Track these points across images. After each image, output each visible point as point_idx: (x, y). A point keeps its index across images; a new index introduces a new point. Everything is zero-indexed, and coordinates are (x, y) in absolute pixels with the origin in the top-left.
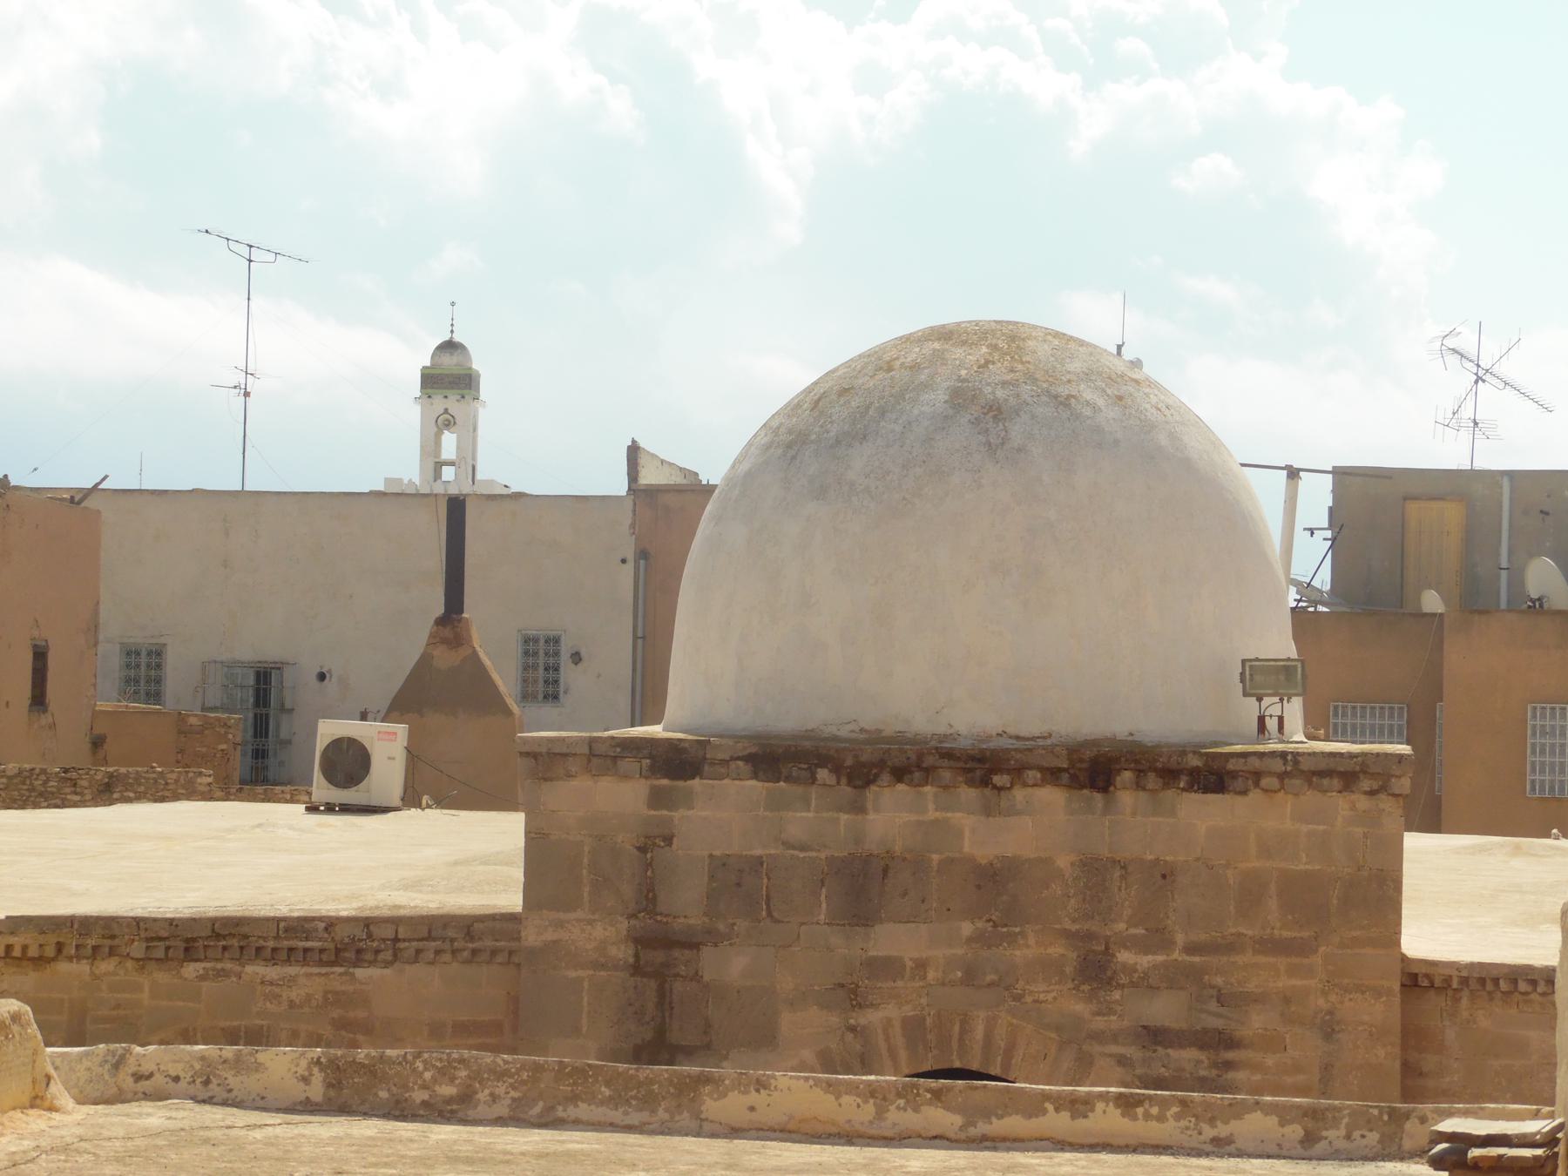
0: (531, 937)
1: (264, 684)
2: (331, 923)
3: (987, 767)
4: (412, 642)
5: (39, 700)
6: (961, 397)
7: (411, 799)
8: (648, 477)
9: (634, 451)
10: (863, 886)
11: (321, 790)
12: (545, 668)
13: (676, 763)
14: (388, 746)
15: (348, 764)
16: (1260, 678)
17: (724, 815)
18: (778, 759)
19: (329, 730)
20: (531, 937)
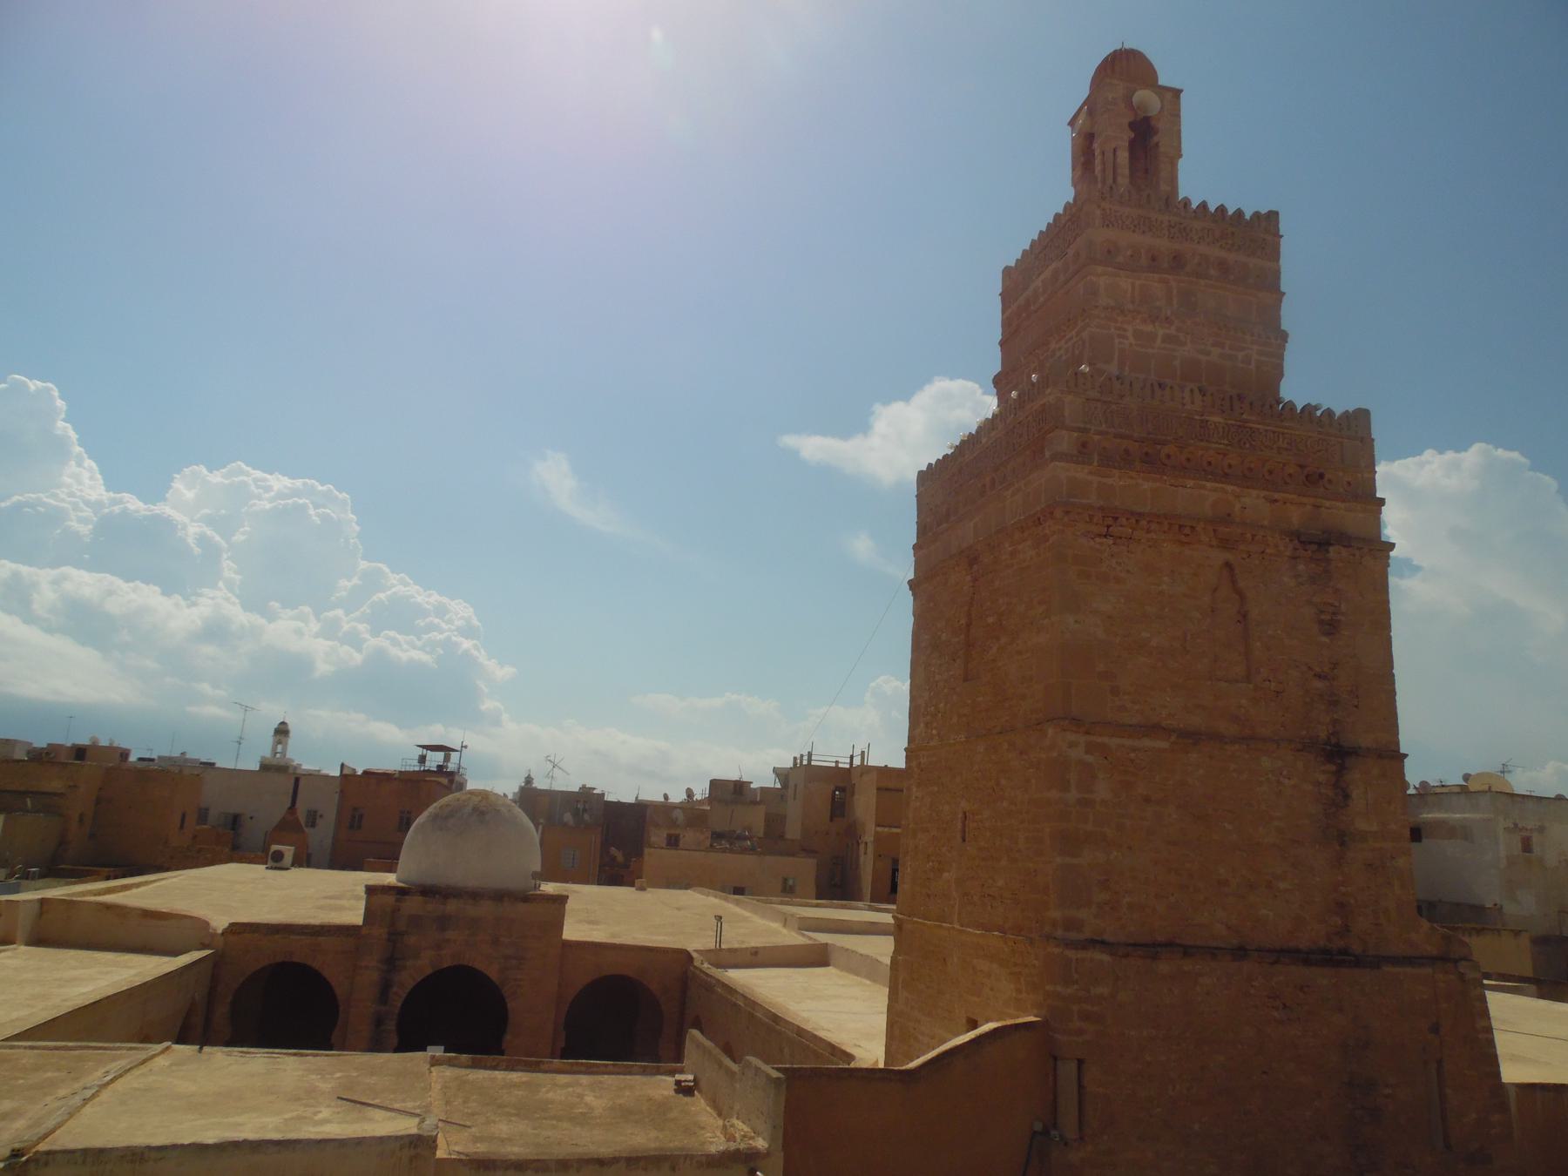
0: (364, 931)
1: (235, 821)
2: (314, 927)
3: (475, 895)
4: (279, 813)
5: (182, 827)
6: (475, 809)
7: (293, 865)
8: (346, 772)
9: (342, 765)
10: (443, 922)
11: (270, 863)
12: (313, 818)
13: (400, 892)
14: (289, 851)
15: (278, 857)
16: (536, 876)
17: (413, 905)
18: (427, 891)
19: (275, 847)
20: (364, 931)
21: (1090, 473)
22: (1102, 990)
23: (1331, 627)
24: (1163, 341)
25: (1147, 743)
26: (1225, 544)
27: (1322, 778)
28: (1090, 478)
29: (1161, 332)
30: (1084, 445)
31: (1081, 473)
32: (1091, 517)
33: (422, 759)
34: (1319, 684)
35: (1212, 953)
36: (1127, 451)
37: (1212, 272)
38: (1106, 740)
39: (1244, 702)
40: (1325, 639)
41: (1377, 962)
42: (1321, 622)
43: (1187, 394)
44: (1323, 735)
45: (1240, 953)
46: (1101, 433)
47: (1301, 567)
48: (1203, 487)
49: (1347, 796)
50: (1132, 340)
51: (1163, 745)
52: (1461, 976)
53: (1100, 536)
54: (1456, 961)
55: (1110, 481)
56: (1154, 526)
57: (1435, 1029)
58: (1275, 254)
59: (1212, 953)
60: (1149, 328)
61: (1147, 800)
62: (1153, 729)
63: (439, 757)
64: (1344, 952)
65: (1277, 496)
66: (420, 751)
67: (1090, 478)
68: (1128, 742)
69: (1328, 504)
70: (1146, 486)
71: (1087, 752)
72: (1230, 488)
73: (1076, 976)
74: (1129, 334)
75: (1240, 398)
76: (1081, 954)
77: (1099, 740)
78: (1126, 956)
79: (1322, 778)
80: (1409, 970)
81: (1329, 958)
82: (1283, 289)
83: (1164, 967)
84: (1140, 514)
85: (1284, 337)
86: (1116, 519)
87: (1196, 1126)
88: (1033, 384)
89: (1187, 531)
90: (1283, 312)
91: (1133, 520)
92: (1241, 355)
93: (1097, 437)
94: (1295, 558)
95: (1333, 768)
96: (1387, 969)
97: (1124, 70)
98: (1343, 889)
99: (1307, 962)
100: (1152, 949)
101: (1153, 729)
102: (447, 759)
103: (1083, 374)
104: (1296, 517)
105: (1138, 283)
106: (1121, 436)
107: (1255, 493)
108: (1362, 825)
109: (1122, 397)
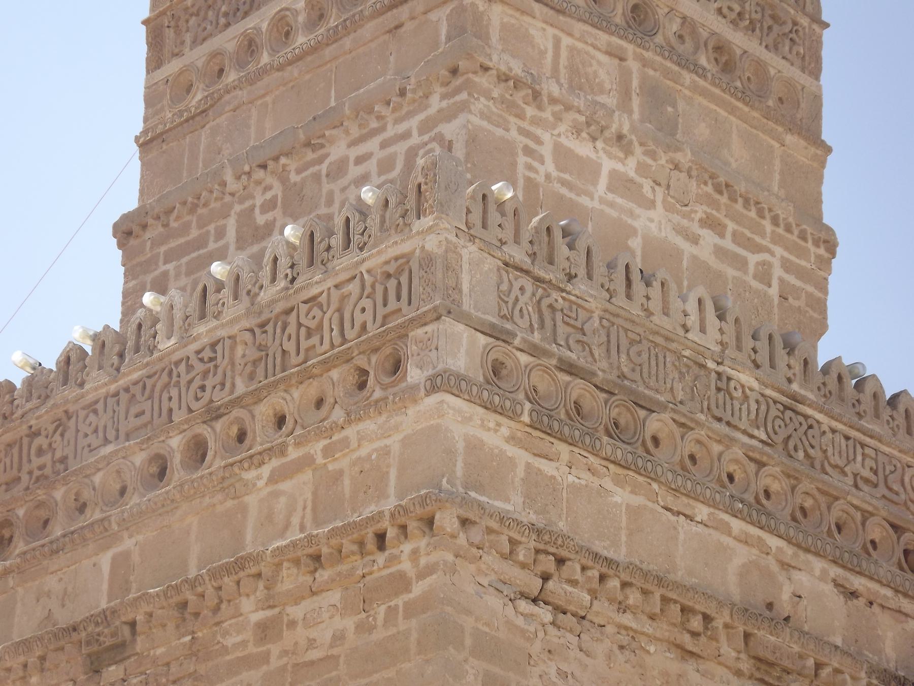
21: (512, 439)
24: (610, 189)
28: (511, 451)
30: (497, 369)
31: (495, 435)
32: (512, 541)
37: (703, 61)
43: (692, 306)
46: (534, 351)
53: (523, 595)
56: (634, 597)
58: (812, 64)
60: (583, 149)
65: (858, 583)
70: (621, 496)
72: (774, 542)
74: (546, 151)
75: (790, 348)
82: (827, 136)
84: (609, 562)
85: (830, 245)
86: (560, 561)
88: (363, 211)
89: (696, 623)
90: (825, 189)
91: (594, 573)
92: (753, 259)
93: (524, 358)
103: (501, 205)
105: (566, 41)
106: (569, 368)
107: (818, 565)
109: (571, 277)
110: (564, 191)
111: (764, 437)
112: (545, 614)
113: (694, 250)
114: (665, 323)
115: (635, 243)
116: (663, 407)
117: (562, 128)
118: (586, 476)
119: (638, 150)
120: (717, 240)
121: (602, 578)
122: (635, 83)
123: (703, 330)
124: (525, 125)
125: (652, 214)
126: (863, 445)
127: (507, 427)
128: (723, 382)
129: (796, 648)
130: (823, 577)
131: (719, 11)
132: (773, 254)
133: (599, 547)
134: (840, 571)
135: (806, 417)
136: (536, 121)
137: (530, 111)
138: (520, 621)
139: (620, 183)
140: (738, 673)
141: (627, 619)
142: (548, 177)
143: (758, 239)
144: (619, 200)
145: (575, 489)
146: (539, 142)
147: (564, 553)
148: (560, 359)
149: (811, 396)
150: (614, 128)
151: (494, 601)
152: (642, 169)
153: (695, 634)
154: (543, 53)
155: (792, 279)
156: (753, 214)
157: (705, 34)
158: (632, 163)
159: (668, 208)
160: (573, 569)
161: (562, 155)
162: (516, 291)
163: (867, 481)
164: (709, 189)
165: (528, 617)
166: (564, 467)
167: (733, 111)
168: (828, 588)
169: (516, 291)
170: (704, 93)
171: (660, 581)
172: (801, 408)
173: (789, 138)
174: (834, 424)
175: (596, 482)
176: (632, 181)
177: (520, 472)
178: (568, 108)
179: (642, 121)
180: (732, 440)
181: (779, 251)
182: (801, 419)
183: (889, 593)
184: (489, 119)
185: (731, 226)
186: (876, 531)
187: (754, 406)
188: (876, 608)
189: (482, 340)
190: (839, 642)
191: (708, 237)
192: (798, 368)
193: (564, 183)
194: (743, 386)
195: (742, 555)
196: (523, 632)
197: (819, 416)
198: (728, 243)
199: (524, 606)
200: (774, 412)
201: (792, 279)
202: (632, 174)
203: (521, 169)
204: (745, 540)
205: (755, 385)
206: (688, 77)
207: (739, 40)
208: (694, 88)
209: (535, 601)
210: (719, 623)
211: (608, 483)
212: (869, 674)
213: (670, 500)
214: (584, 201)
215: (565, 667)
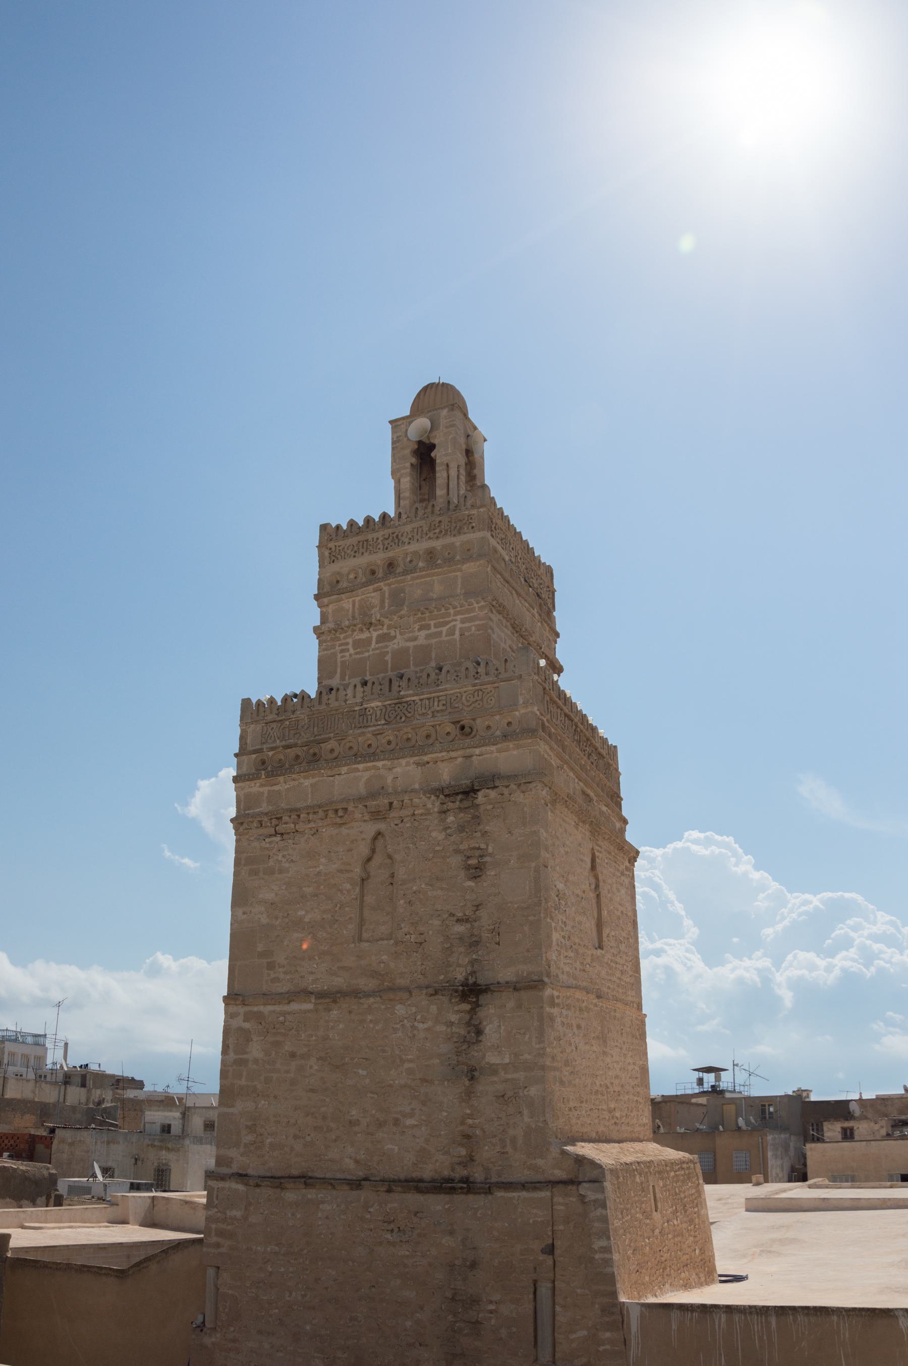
21: (262, 785)
22: (238, 1213)
23: (476, 871)
25: (295, 1006)
26: (377, 815)
27: (454, 1018)
28: (261, 790)
29: (375, 635)
33: (700, 1082)
34: (460, 928)
35: (330, 1183)
36: (297, 757)
38: (261, 1008)
39: (384, 957)
40: (471, 883)
41: (488, 1189)
42: (468, 868)
44: (460, 975)
45: (356, 1184)
46: (272, 749)
47: (451, 819)
48: (358, 770)
49: (479, 1032)
50: (352, 651)
51: (309, 1006)
52: (582, 1197)
54: (580, 1183)
55: (276, 788)
56: (311, 817)
57: (550, 1250)
59: (330, 1183)
61: (293, 1055)
62: (306, 993)
63: (709, 1079)
64: (466, 1180)
65: (426, 758)
66: (697, 1075)
67: (261, 790)
68: (278, 1008)
69: (477, 751)
70: (307, 783)
71: (244, 1021)
72: (380, 764)
73: (216, 1202)
74: (350, 647)
76: (221, 1184)
77: (255, 1009)
78: (258, 1186)
79: (454, 1018)
80: (524, 1194)
81: (443, 1186)
83: (290, 1196)
87: (308, 1327)
91: (294, 816)
92: (444, 629)
93: (271, 753)
94: (445, 812)
95: (466, 1007)
96: (500, 1194)
97: (439, 400)
98: (470, 1121)
99: (419, 1190)
100: (278, 1181)
101: (306, 993)
102: (718, 1079)
104: (446, 772)
107: (403, 762)
108: (492, 1058)
110: (358, 656)
111: (383, 722)
112: (278, 838)
113: (415, 643)
114: (337, 704)
115: (388, 658)
116: (330, 738)
117: (355, 633)
118: (292, 783)
119: (386, 622)
120: (427, 632)
121: (299, 816)
122: (387, 594)
123: (354, 697)
124: (343, 641)
125: (396, 641)
126: (438, 697)
127: (258, 782)
128: (364, 713)
129: (386, 801)
130: (408, 764)
131: (430, 538)
132: (456, 620)
133: (298, 805)
134: (417, 758)
135: (406, 702)
136: (345, 638)
137: (342, 636)
138: (268, 845)
139: (383, 638)
140: (365, 821)
141: (312, 825)
142: (350, 655)
143: (447, 619)
144: (381, 645)
145: (288, 789)
146: (347, 644)
147: (278, 816)
148: (283, 747)
149: (411, 692)
150: (373, 621)
151: (256, 844)
152: (389, 627)
153: (341, 817)
154: (348, 611)
155: (467, 625)
156: (443, 611)
157: (421, 553)
158: (385, 627)
159: (401, 634)
160: (286, 818)
161: (357, 644)
162: (270, 730)
163: (442, 711)
164: (419, 615)
165: (270, 843)
166: (283, 785)
167: (433, 575)
168: (412, 767)
169: (270, 730)
170: (417, 578)
171: (320, 806)
172: (404, 700)
173: (465, 567)
174: (422, 697)
175: (296, 783)
176: (385, 634)
177: (266, 795)
178: (355, 625)
179: (390, 606)
180: (363, 733)
181: (459, 617)
182: (405, 705)
183: (444, 754)
184: (327, 650)
185: (432, 623)
186: (449, 728)
187: (378, 713)
188: (439, 763)
189: (254, 756)
190: (417, 786)
191: (423, 633)
192: (404, 683)
193: (356, 654)
194: (373, 708)
195: (367, 775)
196: (267, 849)
197: (413, 698)
198: (433, 630)
199: (267, 840)
200: (389, 709)
201: (467, 625)
202: (385, 631)
203: (339, 660)
204: (367, 769)
205: (380, 704)
206: (409, 577)
207: (437, 544)
208: (413, 579)
209: (275, 836)
210: (350, 808)
211: (302, 780)
212: (424, 794)
213: (330, 773)
214: (367, 654)
215: (285, 853)
